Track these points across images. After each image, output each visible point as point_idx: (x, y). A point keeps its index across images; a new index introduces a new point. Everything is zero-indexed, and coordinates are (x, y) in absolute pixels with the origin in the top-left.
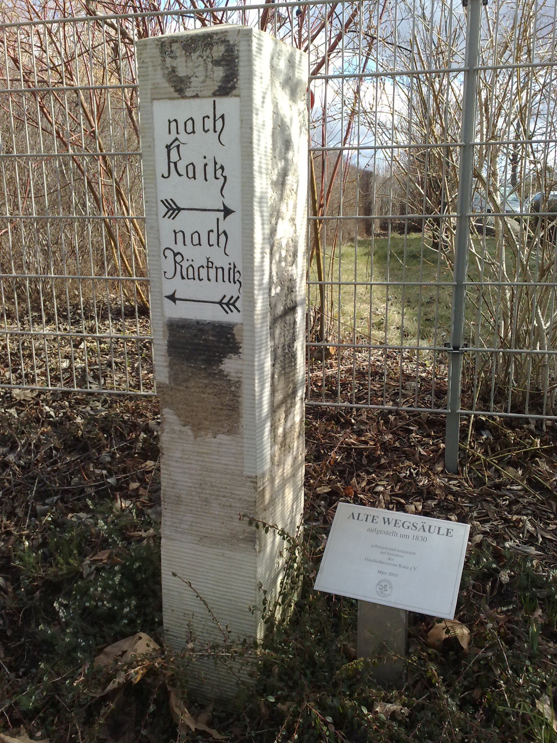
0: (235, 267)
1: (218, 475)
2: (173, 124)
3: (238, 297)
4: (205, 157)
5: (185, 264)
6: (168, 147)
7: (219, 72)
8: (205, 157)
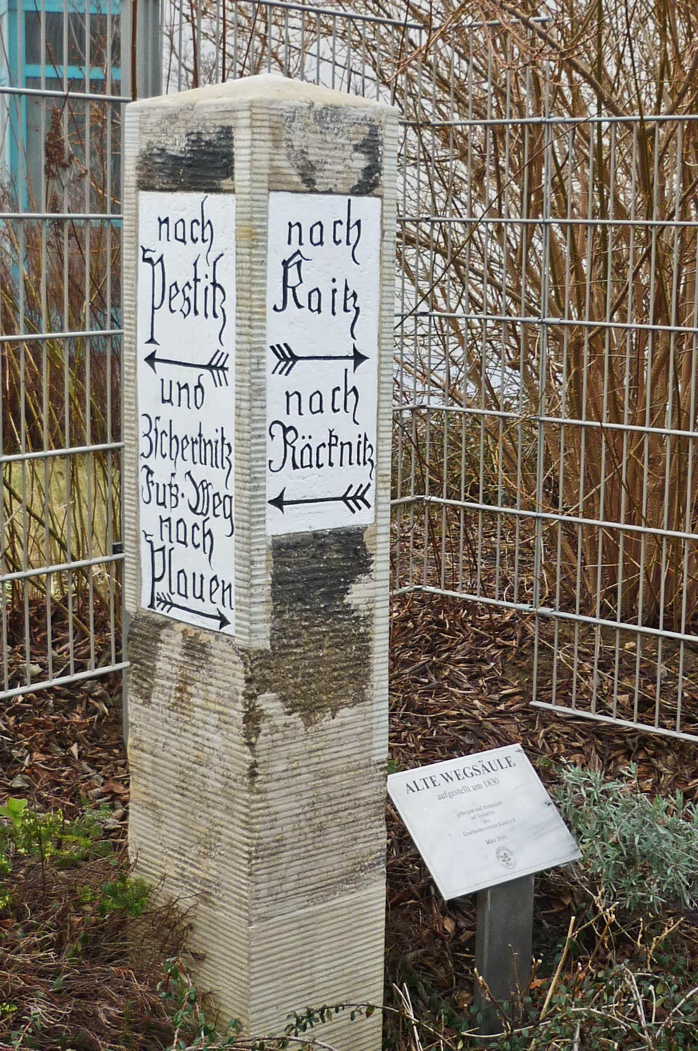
0: (366, 439)
1: (337, 778)
2: (295, 229)
3: (369, 485)
4: (334, 280)
5: (299, 444)
6: (285, 263)
7: (361, 162)
8: (334, 280)
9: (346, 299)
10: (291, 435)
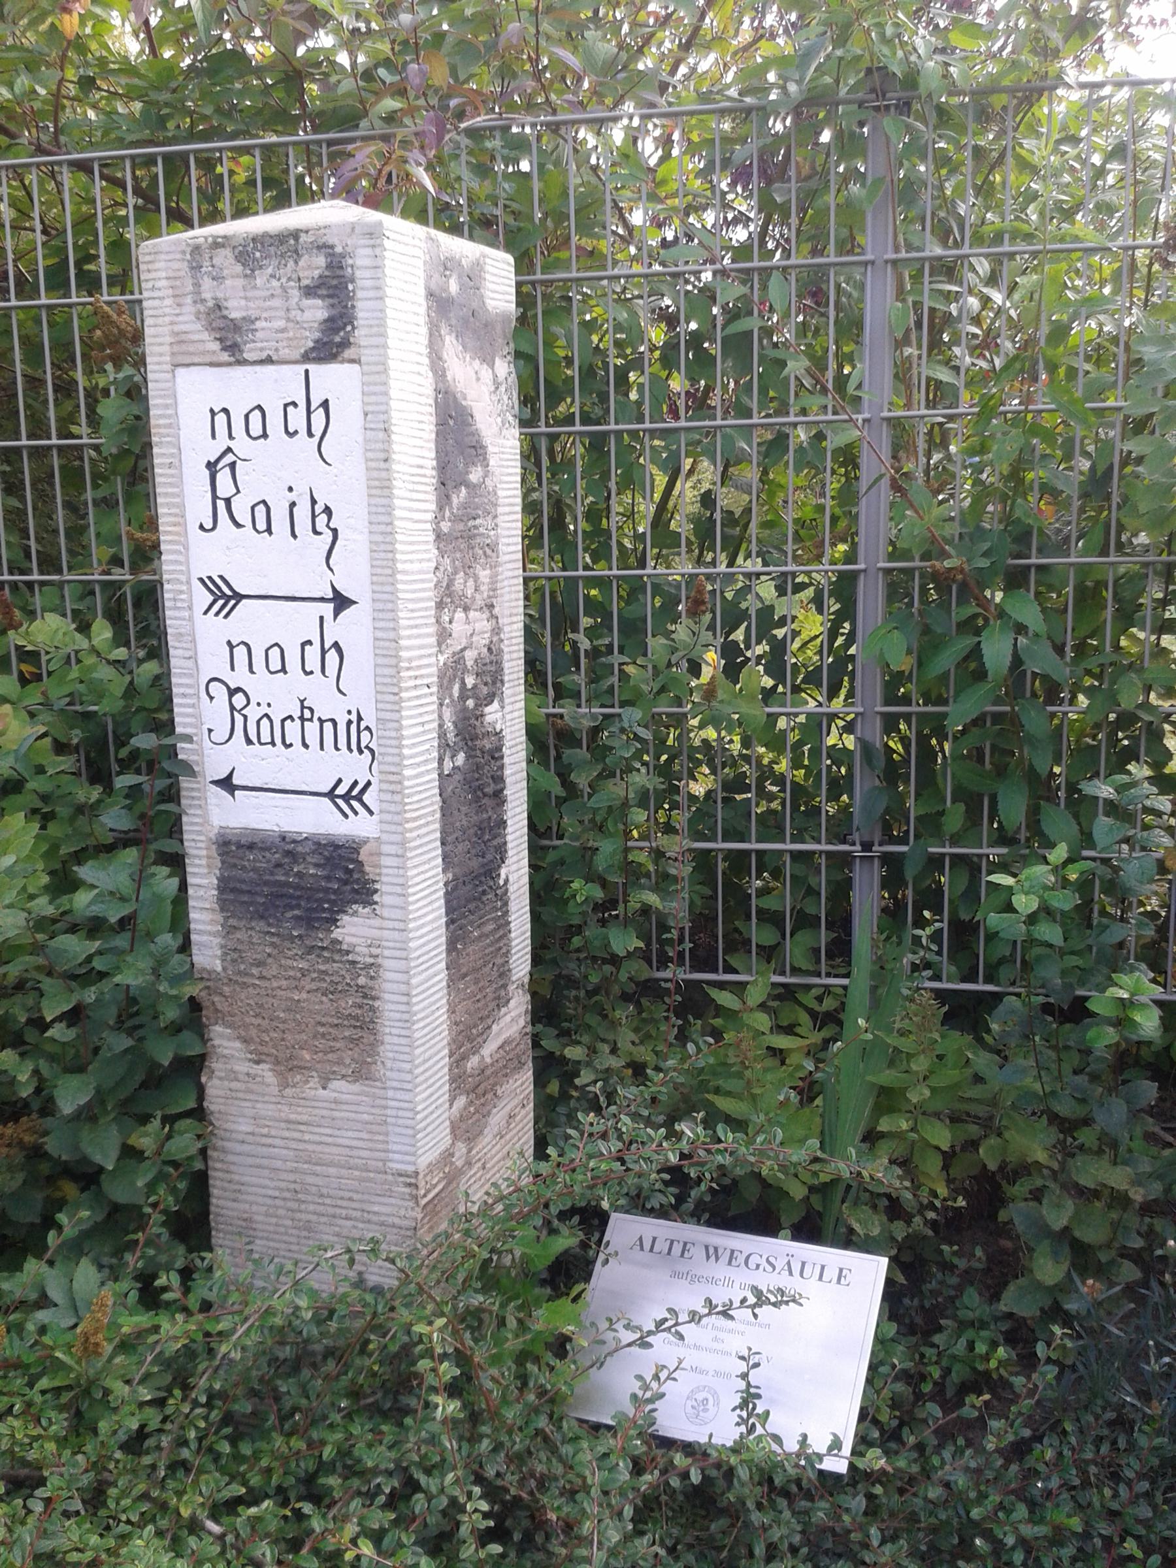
0: (360, 719)
1: (332, 1171)
2: (221, 419)
3: (369, 784)
4: (290, 489)
5: (253, 713)
6: (212, 466)
7: (316, 311)
8: (290, 489)
9: (314, 516)
10: (239, 701)
